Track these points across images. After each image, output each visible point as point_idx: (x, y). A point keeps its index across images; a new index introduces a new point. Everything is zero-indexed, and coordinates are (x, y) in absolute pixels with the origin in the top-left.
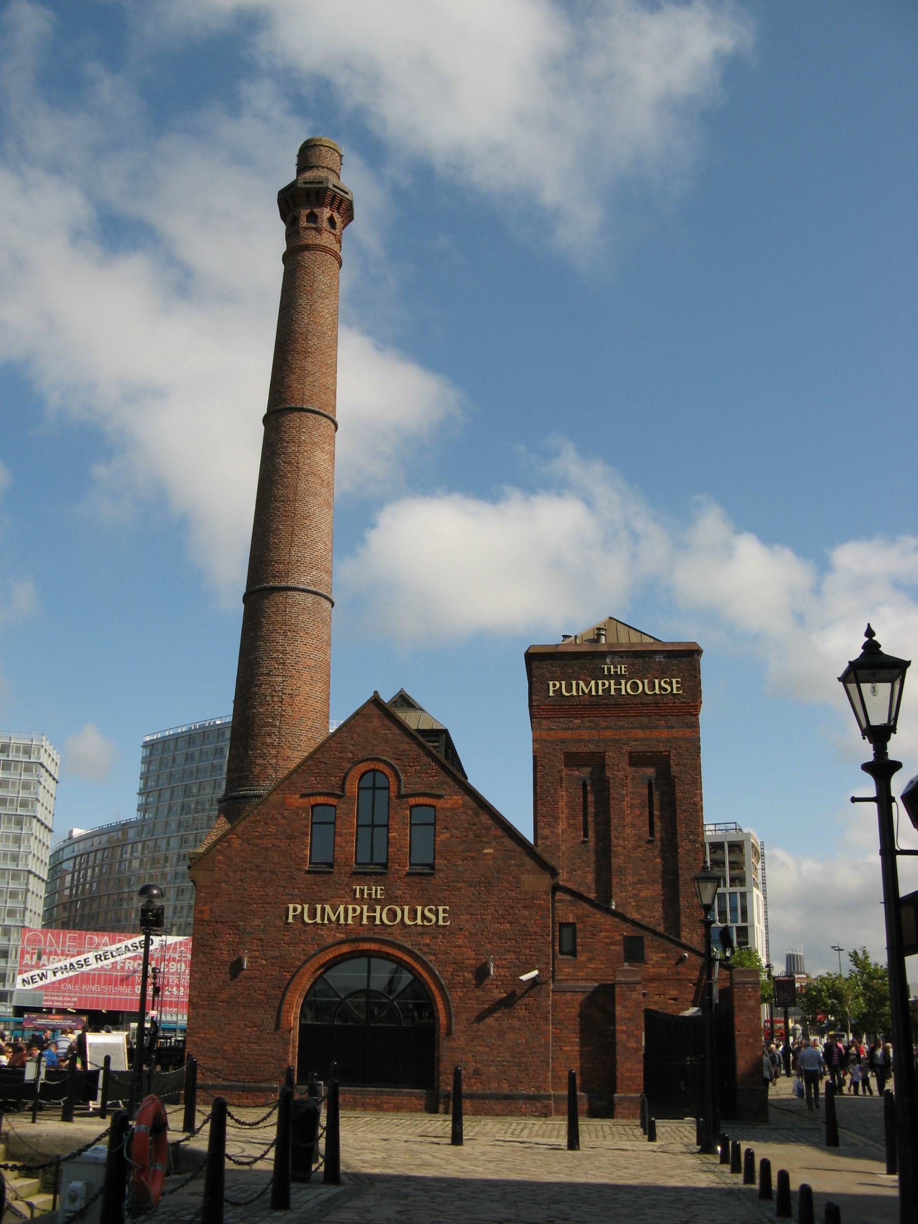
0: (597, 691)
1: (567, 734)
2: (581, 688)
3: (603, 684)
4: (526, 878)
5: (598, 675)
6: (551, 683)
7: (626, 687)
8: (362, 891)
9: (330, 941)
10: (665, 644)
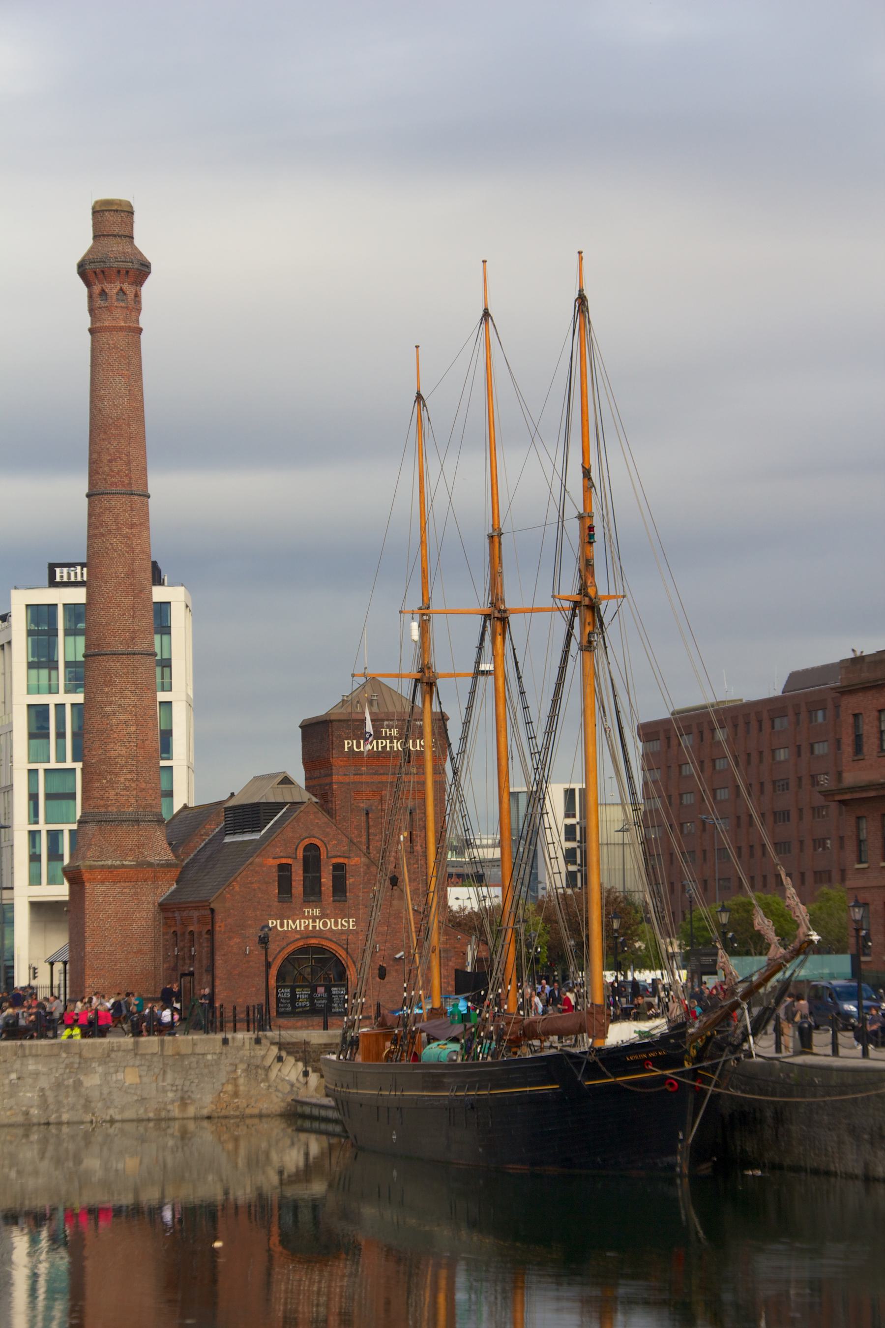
0: (377, 748)
1: (357, 778)
3: (382, 743)
6: (346, 742)
8: (308, 912)
9: (292, 939)
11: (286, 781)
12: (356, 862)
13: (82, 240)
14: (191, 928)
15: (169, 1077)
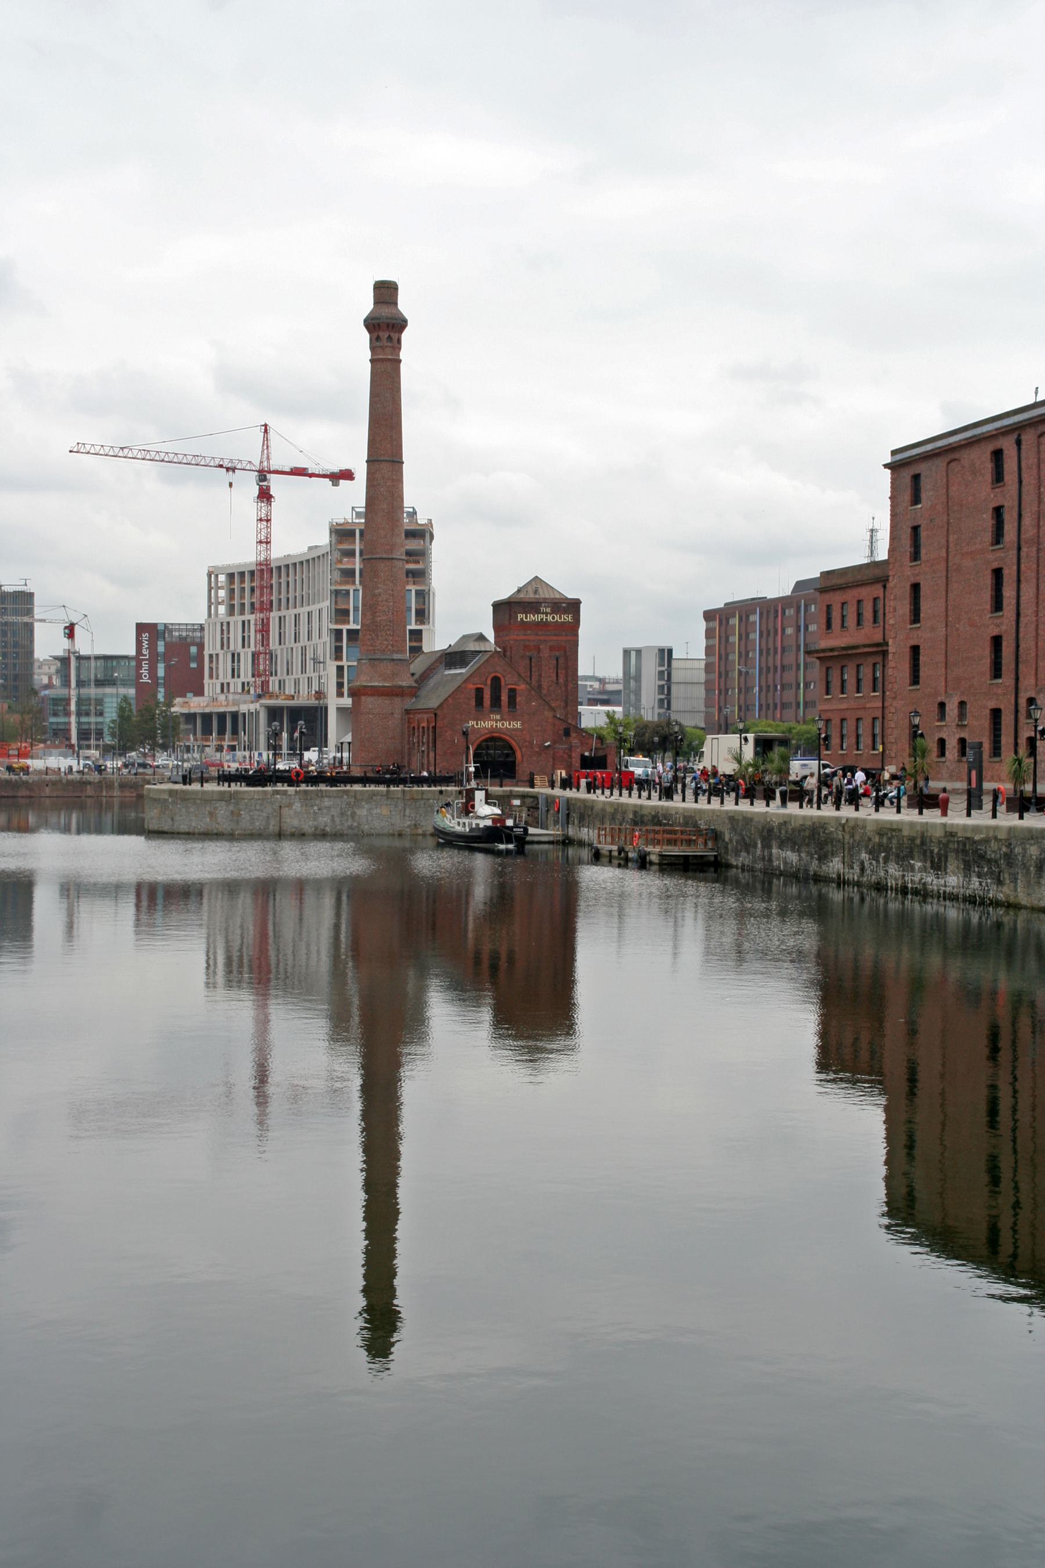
1: (525, 637)
2: (531, 618)
4: (546, 713)
5: (538, 612)
7: (550, 618)
10: (567, 598)
11: (481, 638)
12: (522, 687)
13: (367, 304)
14: (422, 725)
15: (407, 812)
